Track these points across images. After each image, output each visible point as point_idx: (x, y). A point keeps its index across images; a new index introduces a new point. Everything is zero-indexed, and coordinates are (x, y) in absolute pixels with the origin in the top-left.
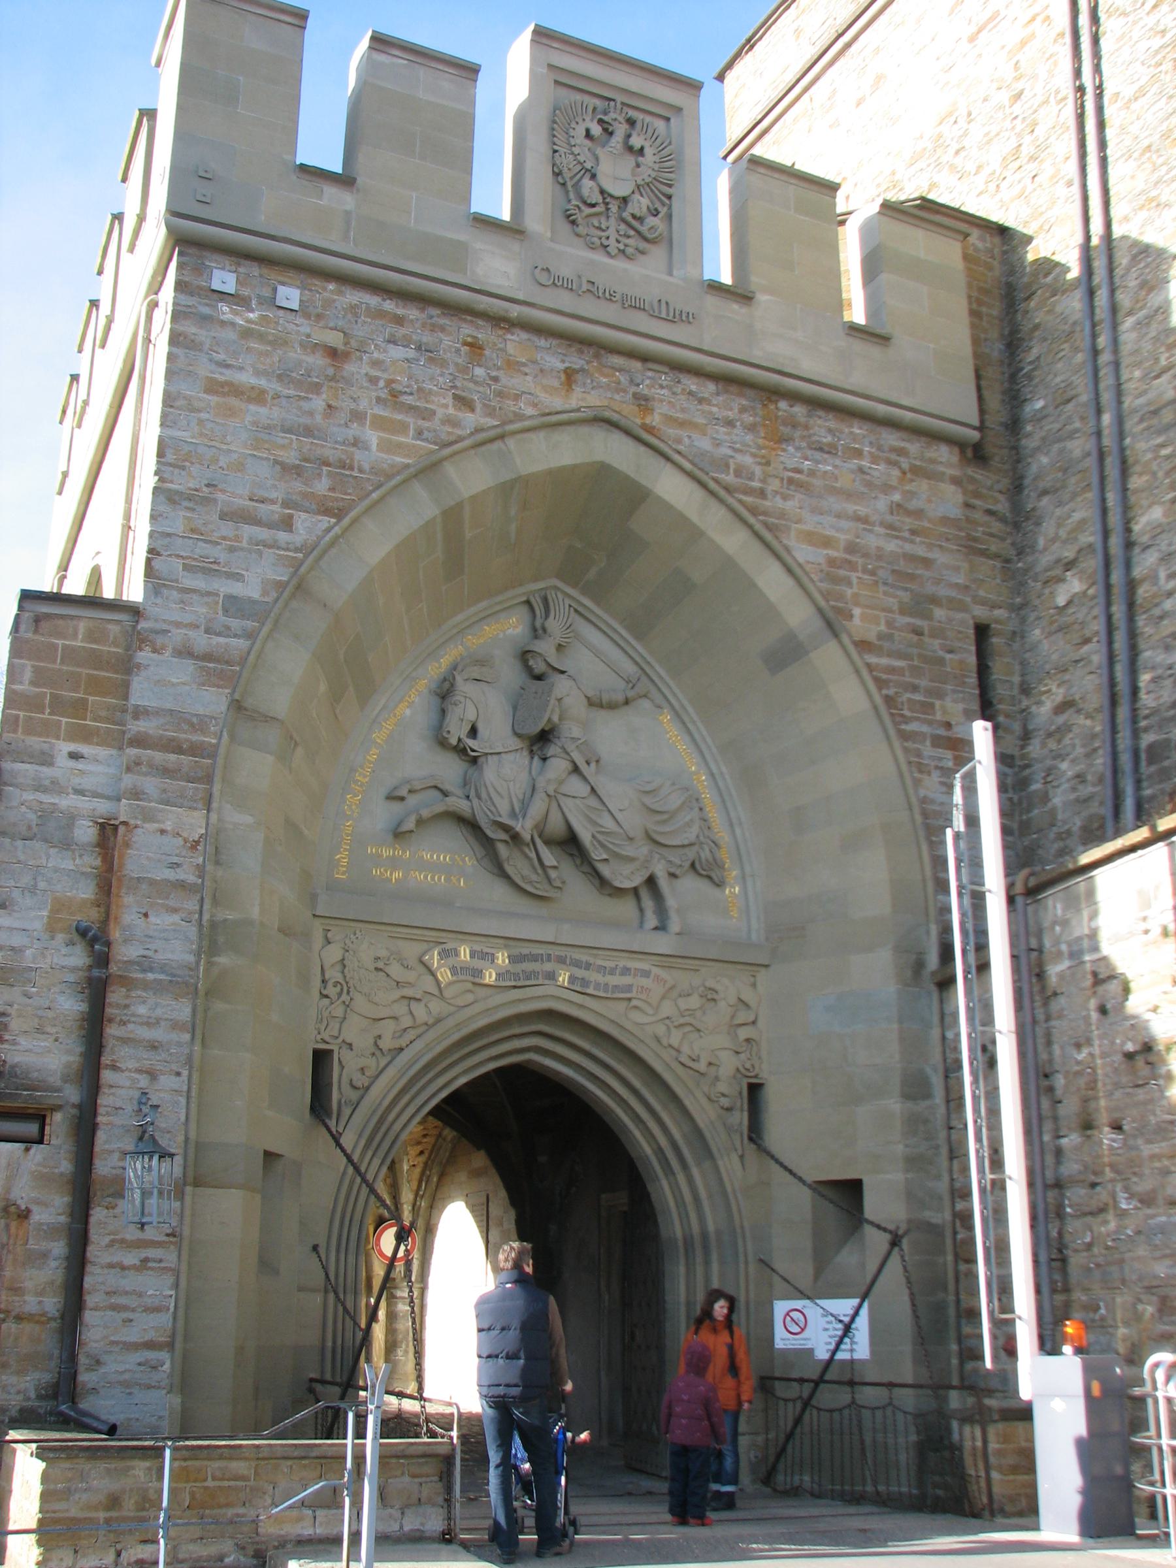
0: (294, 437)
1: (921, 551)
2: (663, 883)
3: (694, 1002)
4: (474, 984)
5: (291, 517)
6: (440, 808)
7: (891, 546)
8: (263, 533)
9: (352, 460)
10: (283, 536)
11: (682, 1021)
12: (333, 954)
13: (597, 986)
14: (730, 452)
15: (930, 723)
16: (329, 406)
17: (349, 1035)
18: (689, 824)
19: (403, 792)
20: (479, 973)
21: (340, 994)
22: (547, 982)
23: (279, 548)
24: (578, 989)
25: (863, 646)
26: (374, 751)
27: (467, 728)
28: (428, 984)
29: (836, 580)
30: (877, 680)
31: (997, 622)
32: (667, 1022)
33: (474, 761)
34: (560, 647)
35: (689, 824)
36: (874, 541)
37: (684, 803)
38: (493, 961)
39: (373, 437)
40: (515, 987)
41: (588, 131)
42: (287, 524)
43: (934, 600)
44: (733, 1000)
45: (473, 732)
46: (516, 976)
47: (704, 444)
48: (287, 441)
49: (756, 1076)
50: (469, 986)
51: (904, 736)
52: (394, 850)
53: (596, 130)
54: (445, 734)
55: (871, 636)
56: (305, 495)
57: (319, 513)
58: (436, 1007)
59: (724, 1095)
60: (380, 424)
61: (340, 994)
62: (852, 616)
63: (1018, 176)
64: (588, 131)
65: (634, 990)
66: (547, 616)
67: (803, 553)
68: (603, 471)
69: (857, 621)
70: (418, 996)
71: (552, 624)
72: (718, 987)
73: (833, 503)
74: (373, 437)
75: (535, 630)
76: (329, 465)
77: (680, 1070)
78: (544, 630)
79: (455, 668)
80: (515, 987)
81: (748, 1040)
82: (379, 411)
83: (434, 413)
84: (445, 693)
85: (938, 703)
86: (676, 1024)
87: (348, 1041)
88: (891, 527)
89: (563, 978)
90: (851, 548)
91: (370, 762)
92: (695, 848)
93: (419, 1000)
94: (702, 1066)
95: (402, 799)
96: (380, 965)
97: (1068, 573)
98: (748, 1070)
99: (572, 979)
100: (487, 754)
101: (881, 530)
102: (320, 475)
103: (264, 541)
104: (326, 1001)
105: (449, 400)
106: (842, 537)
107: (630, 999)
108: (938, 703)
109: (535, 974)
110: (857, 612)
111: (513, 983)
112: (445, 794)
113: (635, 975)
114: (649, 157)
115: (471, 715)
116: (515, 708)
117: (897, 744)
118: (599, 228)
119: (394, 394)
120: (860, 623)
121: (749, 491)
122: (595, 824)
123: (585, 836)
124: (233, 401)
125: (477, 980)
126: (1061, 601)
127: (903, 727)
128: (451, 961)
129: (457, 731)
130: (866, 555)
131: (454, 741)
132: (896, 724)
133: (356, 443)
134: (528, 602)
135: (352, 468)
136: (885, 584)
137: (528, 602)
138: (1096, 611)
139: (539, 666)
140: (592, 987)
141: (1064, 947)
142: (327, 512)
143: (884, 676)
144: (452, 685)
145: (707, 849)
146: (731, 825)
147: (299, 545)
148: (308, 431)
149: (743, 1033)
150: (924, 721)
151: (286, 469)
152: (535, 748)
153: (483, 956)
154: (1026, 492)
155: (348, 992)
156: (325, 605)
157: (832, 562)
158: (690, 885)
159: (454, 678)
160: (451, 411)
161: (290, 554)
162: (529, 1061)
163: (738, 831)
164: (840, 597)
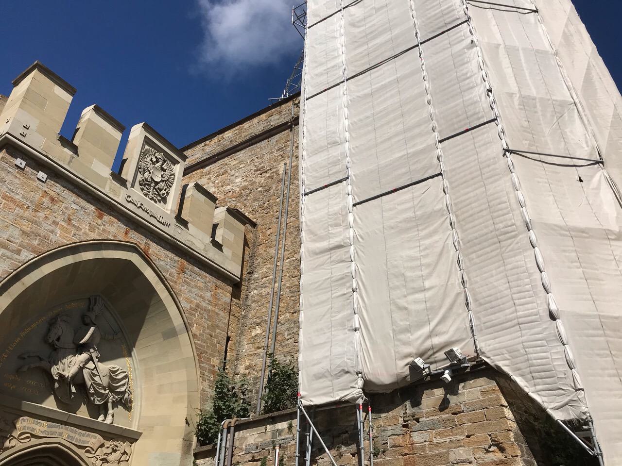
0: (30, 223)
1: (217, 310)
4: (31, 434)
5: (20, 250)
6: (38, 365)
7: (209, 307)
8: (9, 254)
9: (49, 237)
10: (15, 256)
14: (169, 267)
15: (209, 364)
16: (46, 217)
18: (124, 385)
19: (26, 356)
23: (13, 260)
24: (70, 441)
25: (195, 336)
26: (18, 339)
27: (57, 337)
29: (191, 314)
30: (196, 348)
31: (233, 336)
32: (98, 457)
33: (55, 349)
34: (96, 316)
35: (124, 385)
36: (204, 305)
39: (59, 232)
41: (152, 158)
42: (18, 252)
43: (218, 326)
45: (58, 339)
47: (162, 263)
48: (27, 224)
51: (201, 367)
52: (15, 377)
53: (154, 159)
54: (48, 338)
55: (198, 333)
56: (28, 244)
57: (32, 252)
60: (62, 228)
62: (193, 326)
63: (262, 211)
64: (152, 158)
66: (94, 305)
67: (184, 304)
68: (129, 263)
69: (194, 328)
71: (96, 308)
72: (118, 445)
73: (195, 290)
74: (59, 232)
75: (89, 308)
76: (40, 236)
78: (93, 309)
79: (58, 315)
82: (63, 223)
83: (81, 229)
84: (52, 323)
85: (212, 359)
88: (210, 301)
90: (198, 305)
91: (16, 343)
95: (24, 358)
97: (257, 327)
99: (69, 436)
100: (61, 348)
101: (207, 302)
102: (36, 239)
103: (8, 256)
105: (87, 227)
106: (195, 301)
107: (87, 447)
108: (212, 359)
110: (195, 325)
112: (41, 359)
113: (91, 438)
114: (167, 173)
115: (60, 333)
116: (75, 334)
117: (198, 369)
118: (147, 188)
119: (70, 220)
120: (194, 329)
121: (172, 281)
122: (93, 380)
124: (11, 205)
125: (33, 433)
126: (253, 334)
127: (201, 364)
129: (52, 338)
130: (201, 309)
131: (50, 341)
132: (199, 363)
133: (52, 232)
134: (89, 299)
135: (48, 240)
136: (205, 319)
137: (89, 299)
138: (264, 340)
139: (87, 321)
141: (244, 447)
142: (34, 252)
143: (199, 347)
144: (56, 321)
147: (20, 261)
148: (36, 223)
150: (207, 364)
151: (24, 232)
152: (79, 349)
154: (248, 299)
156: (23, 284)
157: (191, 308)
159: (58, 319)
160: (87, 231)
161: (16, 263)
164: (192, 320)
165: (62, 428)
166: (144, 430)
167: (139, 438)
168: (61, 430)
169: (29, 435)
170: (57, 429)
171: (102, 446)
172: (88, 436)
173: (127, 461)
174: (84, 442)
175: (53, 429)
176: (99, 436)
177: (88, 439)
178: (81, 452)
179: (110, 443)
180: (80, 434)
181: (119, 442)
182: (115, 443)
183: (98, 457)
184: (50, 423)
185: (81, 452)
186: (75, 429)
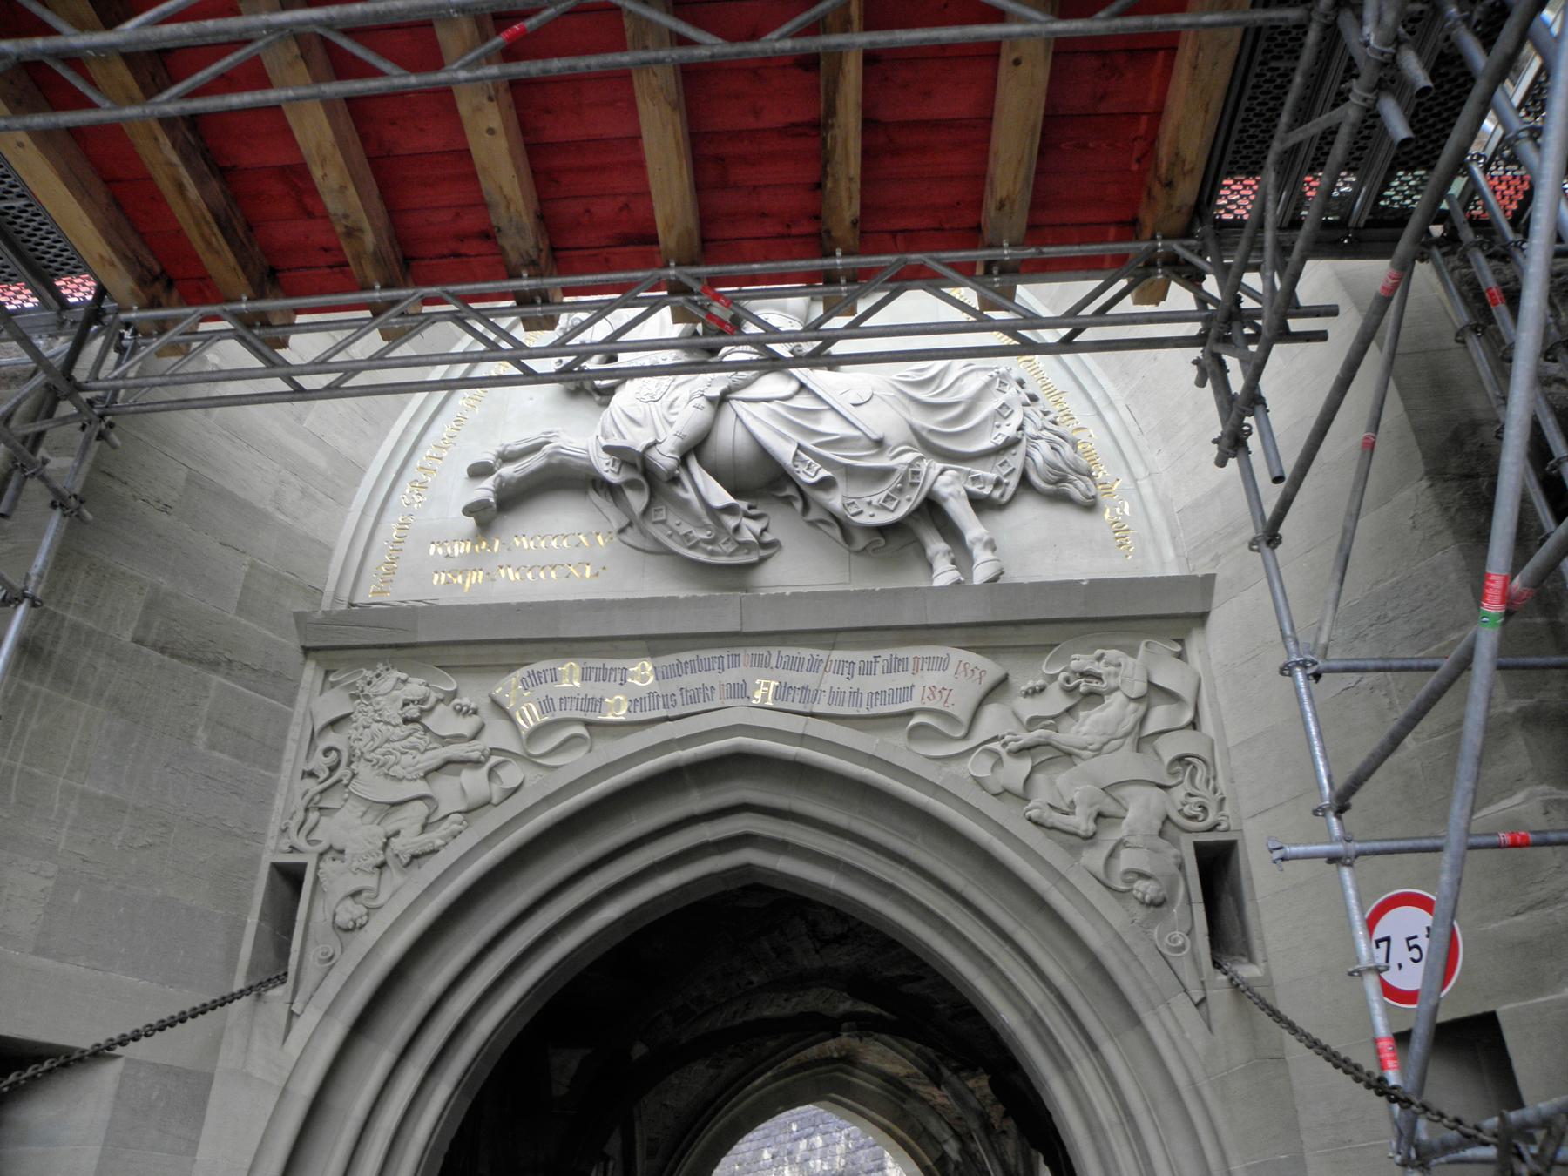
2: (959, 510)
3: (1055, 702)
4: (588, 724)
11: (1027, 737)
12: (332, 704)
13: (836, 696)
17: (329, 830)
18: (1003, 412)
20: (597, 703)
21: (333, 769)
22: (729, 702)
28: (498, 735)
32: (996, 746)
37: (987, 385)
38: (624, 682)
40: (667, 719)
44: (1139, 688)
46: (669, 700)
49: (1213, 829)
50: (581, 730)
58: (511, 775)
59: (1142, 876)
61: (333, 769)
65: (917, 693)
70: (475, 755)
77: (1034, 837)
80: (667, 719)
81: (1181, 759)
86: (1012, 746)
87: (338, 846)
89: (763, 691)
92: (1021, 449)
93: (477, 763)
94: (1081, 821)
96: (413, 711)
98: (1193, 818)
99: (782, 691)
104: (310, 782)
107: (910, 714)
109: (706, 691)
111: (662, 713)
113: (916, 671)
123: (784, 450)
125: (591, 716)
128: (543, 690)
140: (824, 698)
145: (1043, 445)
146: (1099, 413)
149: (1169, 749)
153: (605, 674)
155: (350, 763)
158: (1030, 518)
162: (748, 868)
163: (1110, 417)
165: (735, 665)
166: (1217, 558)
167: (1210, 604)
168: (732, 676)
169: (581, 730)
170: (713, 674)
171: (999, 688)
172: (894, 666)
173: (1194, 725)
174: (893, 696)
175: (691, 680)
176: (958, 656)
177: (901, 680)
178: (893, 746)
179: (1047, 667)
180: (848, 669)
181: (1098, 652)
182: (1081, 661)
183: (996, 746)
184: (670, 659)
185: (893, 746)
186: (806, 653)
